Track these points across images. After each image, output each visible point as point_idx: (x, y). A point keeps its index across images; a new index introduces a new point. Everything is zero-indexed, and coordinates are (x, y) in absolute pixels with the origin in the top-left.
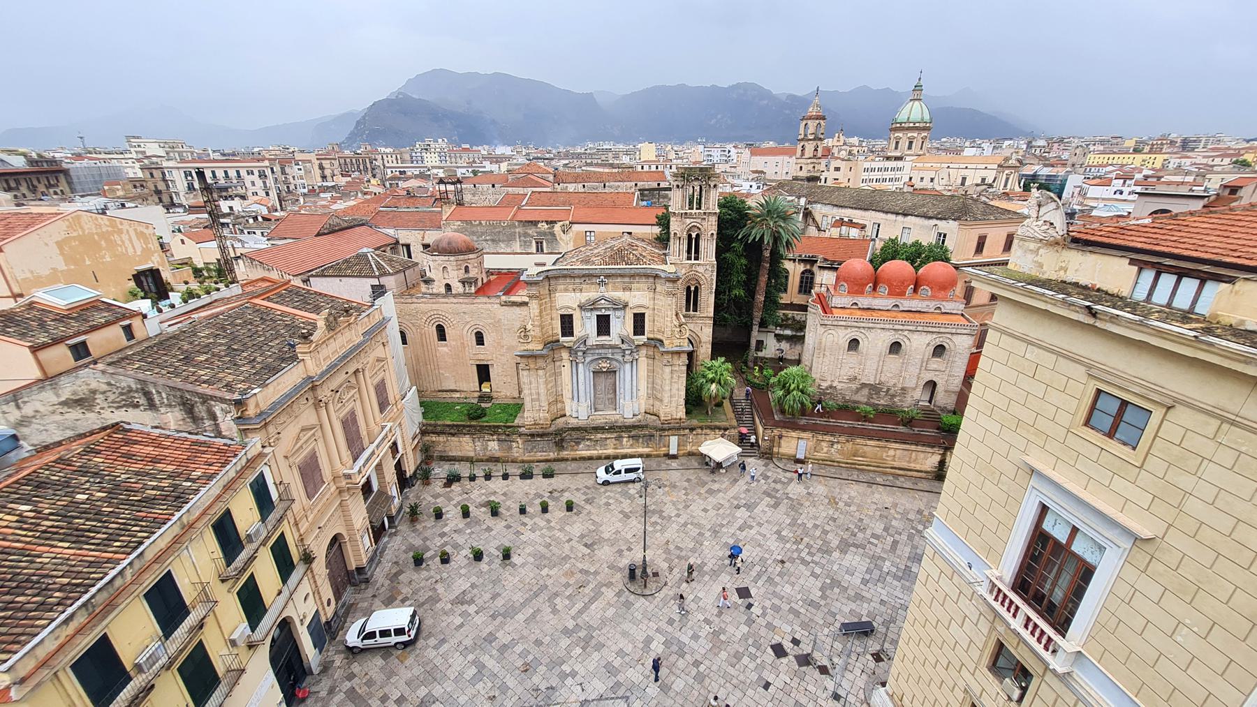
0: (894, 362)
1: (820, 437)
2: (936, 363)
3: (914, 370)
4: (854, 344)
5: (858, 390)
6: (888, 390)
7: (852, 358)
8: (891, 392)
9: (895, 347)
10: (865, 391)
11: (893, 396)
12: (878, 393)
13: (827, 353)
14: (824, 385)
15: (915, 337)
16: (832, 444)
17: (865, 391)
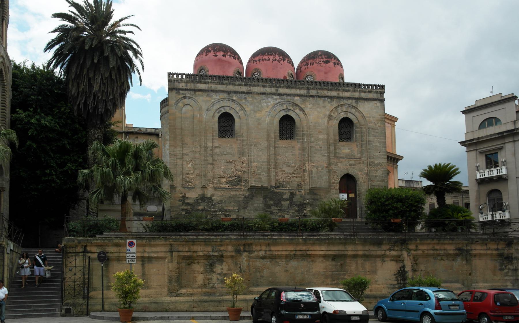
0: (289, 151)
1: (185, 251)
2: (345, 149)
3: (320, 159)
4: (226, 124)
5: (248, 200)
6: (292, 195)
7: (228, 146)
9: (287, 126)
10: (258, 202)
12: (278, 203)
13: (188, 140)
14: (193, 195)
15: (309, 105)
16: (211, 262)
17: (258, 202)
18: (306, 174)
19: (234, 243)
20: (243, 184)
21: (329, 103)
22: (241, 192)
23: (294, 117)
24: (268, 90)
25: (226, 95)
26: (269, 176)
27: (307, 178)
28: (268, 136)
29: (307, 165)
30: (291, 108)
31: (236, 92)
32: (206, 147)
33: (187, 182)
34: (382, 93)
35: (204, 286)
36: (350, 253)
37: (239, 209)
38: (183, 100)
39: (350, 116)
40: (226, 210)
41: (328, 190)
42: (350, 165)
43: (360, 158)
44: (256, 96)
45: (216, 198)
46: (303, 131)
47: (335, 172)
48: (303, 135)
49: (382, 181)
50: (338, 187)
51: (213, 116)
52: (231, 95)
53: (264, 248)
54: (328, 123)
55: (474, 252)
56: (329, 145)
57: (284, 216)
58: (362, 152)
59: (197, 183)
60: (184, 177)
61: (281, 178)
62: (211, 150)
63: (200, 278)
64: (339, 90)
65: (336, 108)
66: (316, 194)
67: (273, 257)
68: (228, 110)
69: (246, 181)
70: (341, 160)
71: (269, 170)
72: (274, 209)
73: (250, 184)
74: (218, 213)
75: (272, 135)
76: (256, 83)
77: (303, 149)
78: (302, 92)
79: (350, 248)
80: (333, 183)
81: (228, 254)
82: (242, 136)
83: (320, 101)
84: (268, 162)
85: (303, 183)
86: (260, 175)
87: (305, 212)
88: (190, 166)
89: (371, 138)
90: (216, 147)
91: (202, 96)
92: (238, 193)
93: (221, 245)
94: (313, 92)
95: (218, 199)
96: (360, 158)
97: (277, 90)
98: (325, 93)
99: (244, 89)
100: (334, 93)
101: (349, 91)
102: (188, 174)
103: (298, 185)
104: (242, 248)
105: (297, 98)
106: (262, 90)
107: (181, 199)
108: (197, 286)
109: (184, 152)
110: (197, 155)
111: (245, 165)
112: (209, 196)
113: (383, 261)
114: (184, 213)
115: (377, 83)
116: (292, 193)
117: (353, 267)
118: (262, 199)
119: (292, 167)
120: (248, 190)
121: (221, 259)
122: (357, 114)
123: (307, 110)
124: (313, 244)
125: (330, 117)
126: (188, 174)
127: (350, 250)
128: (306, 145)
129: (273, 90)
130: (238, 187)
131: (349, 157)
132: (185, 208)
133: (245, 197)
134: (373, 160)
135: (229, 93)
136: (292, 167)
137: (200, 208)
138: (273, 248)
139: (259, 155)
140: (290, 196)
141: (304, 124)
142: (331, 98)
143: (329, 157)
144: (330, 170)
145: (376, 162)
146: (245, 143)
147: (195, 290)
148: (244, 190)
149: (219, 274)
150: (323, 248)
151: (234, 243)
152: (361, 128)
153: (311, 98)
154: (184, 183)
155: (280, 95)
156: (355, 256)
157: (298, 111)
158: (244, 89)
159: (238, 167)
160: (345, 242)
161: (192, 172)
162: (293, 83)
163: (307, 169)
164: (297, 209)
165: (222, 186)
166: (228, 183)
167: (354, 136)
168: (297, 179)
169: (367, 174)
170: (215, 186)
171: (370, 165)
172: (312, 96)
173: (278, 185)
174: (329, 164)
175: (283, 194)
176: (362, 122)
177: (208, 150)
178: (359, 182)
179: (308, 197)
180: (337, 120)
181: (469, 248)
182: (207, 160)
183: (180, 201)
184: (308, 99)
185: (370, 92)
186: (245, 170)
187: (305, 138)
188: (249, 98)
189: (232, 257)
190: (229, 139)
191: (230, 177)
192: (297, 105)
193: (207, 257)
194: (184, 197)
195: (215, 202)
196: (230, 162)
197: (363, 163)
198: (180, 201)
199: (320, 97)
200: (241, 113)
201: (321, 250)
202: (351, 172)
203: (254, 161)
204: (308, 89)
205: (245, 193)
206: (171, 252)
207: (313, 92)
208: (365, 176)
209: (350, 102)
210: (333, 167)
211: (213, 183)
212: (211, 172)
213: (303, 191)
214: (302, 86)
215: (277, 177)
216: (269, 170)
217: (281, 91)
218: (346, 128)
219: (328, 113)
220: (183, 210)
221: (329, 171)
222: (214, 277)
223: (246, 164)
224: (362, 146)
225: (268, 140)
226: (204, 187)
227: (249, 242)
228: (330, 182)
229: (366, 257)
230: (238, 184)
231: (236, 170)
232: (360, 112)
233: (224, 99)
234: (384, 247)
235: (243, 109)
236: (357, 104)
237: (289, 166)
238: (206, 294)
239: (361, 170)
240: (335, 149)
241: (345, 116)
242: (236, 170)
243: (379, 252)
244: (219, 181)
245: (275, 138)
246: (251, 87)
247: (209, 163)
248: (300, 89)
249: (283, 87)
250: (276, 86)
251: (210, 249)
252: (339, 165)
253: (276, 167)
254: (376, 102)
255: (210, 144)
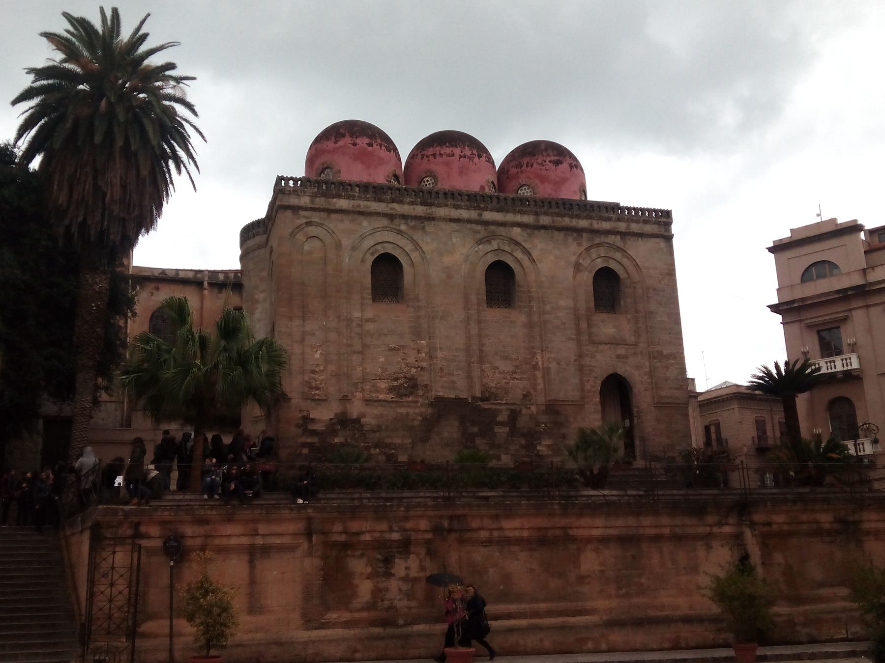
0: (506, 329)
2: (607, 327)
3: (562, 346)
5: (430, 425)
6: (514, 415)
7: (392, 318)
8: (523, 422)
10: (450, 429)
11: (532, 437)
14: (323, 414)
15: (539, 245)
16: (386, 555)
17: (450, 429)
18: (539, 374)
19: (431, 513)
20: (420, 393)
21: (575, 240)
22: (416, 409)
23: (512, 264)
24: (464, 214)
25: (385, 222)
26: (469, 377)
27: (540, 381)
28: (467, 300)
29: (539, 357)
30: (507, 248)
31: (404, 217)
32: (349, 320)
33: (311, 388)
34: (669, 224)
35: (371, 606)
36: (649, 531)
37: (413, 443)
38: (306, 229)
39: (613, 265)
40: (388, 446)
41: (579, 405)
42: (618, 357)
43: (636, 344)
44: (442, 225)
45: (369, 421)
46: (529, 291)
47: (591, 370)
48: (531, 299)
49: (678, 389)
50: (598, 399)
51: (363, 260)
52: (397, 221)
53: (486, 522)
54: (574, 277)
55: (866, 526)
56: (577, 319)
57: (498, 458)
58: (637, 333)
59: (332, 389)
60: (306, 378)
61: (493, 381)
62: (359, 326)
63: (365, 589)
64: (591, 218)
65: (588, 249)
66: (557, 413)
67: (505, 542)
68: (389, 249)
69: (426, 386)
70: (601, 347)
71: (469, 365)
72: (478, 441)
73: (433, 393)
74: (373, 451)
75: (473, 298)
76: (441, 200)
77: (530, 325)
78: (527, 219)
79: (647, 521)
80: (589, 391)
81: (420, 536)
82: (417, 299)
83: (559, 236)
84: (468, 349)
85: (532, 391)
86: (452, 375)
87: (539, 448)
88: (317, 356)
89: (653, 307)
90: (369, 320)
91: (342, 221)
92: (411, 411)
93: (406, 519)
94: (545, 220)
95: (374, 422)
96: (636, 344)
97: (480, 215)
98: (566, 221)
99: (420, 210)
100: (583, 223)
101: (609, 219)
102: (313, 372)
103: (524, 396)
104: (446, 524)
105: (517, 230)
106: (455, 213)
107: (300, 422)
108: (359, 606)
109: (308, 328)
110: (333, 336)
111: (424, 355)
112: (355, 417)
113: (709, 547)
114: (305, 451)
115: (658, 207)
116: (513, 412)
117: (655, 561)
118: (456, 423)
119: (511, 360)
120: (431, 404)
121: (405, 546)
122: (625, 261)
123: (535, 254)
124: (581, 515)
125: (578, 267)
126: (313, 372)
127: (647, 524)
128: (535, 318)
129: (473, 214)
130: (411, 398)
131: (615, 342)
132: (309, 440)
133: (425, 419)
134: (658, 348)
135: (391, 217)
136: (511, 360)
137: (337, 440)
138: (506, 524)
139: (451, 336)
140: (509, 416)
141: (532, 277)
142: (579, 231)
143: (579, 342)
144: (583, 366)
145: (665, 352)
146: (422, 313)
147: (357, 615)
148: (421, 405)
149: (402, 579)
150: (599, 522)
151: (431, 513)
152: (635, 288)
153: (542, 231)
154: (306, 389)
155: (486, 223)
156: (657, 539)
157: (519, 254)
158: (420, 210)
159: (411, 360)
160: (637, 508)
161: (322, 368)
162: (510, 202)
163: (540, 364)
164: (523, 442)
165: (381, 397)
166: (391, 390)
167: (622, 302)
168: (522, 384)
169: (651, 374)
170: (367, 396)
171: (654, 358)
172: (544, 227)
173: (487, 394)
174: (580, 356)
175: (494, 413)
176: (636, 276)
177: (354, 324)
178: (635, 390)
179: (543, 418)
180: (590, 272)
181: (857, 517)
182: (351, 346)
183: (297, 426)
184: (536, 232)
185: (646, 222)
186: (424, 364)
187: (534, 304)
188: (430, 227)
189: (428, 542)
190: (394, 305)
191: (396, 379)
192: (517, 244)
193: (380, 545)
194: (307, 419)
195: (366, 428)
196: (394, 349)
197: (641, 354)
198: (297, 426)
199: (560, 229)
200: (415, 256)
201: (595, 526)
202: (620, 371)
203: (441, 349)
204: (536, 214)
205: (423, 410)
206: (309, 534)
207: (545, 220)
208: (646, 377)
209: (611, 239)
210: (587, 361)
211: (363, 390)
212: (359, 369)
213: (533, 408)
214: (524, 209)
215: (485, 380)
216: (469, 365)
217: (488, 216)
218: (608, 288)
219: (573, 259)
220: (304, 445)
221: (581, 369)
222: (394, 586)
223: (426, 353)
224: (637, 322)
225: (466, 308)
226: (345, 399)
227: (459, 512)
228: (582, 390)
229: (678, 539)
230: (411, 393)
231: (407, 365)
232: (630, 258)
233: (384, 229)
234: (710, 519)
235: (417, 246)
236: (625, 243)
237: (506, 358)
238: (373, 623)
239: (638, 367)
240: (589, 326)
241: (604, 265)
242: (407, 365)
243: (701, 530)
244: (374, 386)
245: (479, 304)
246: (433, 208)
247: (354, 352)
248: (521, 212)
249: (492, 210)
250: (478, 208)
251: (384, 526)
252: (599, 356)
253: (482, 359)
254: (657, 240)
255: (357, 314)
